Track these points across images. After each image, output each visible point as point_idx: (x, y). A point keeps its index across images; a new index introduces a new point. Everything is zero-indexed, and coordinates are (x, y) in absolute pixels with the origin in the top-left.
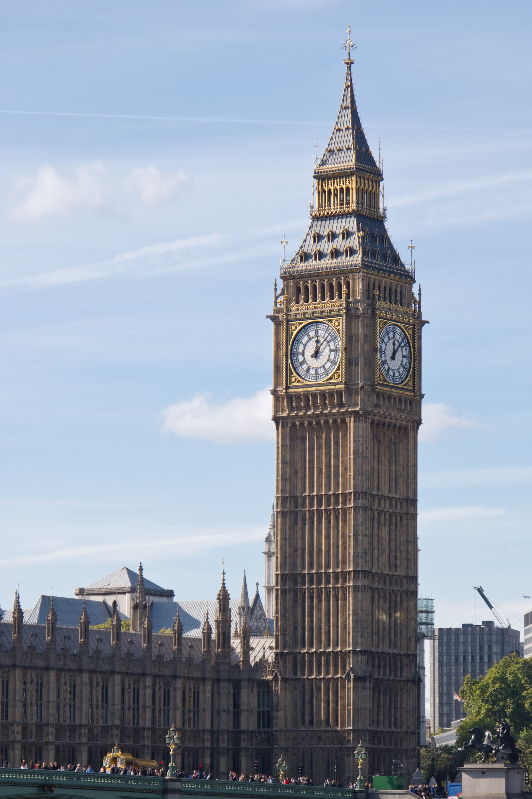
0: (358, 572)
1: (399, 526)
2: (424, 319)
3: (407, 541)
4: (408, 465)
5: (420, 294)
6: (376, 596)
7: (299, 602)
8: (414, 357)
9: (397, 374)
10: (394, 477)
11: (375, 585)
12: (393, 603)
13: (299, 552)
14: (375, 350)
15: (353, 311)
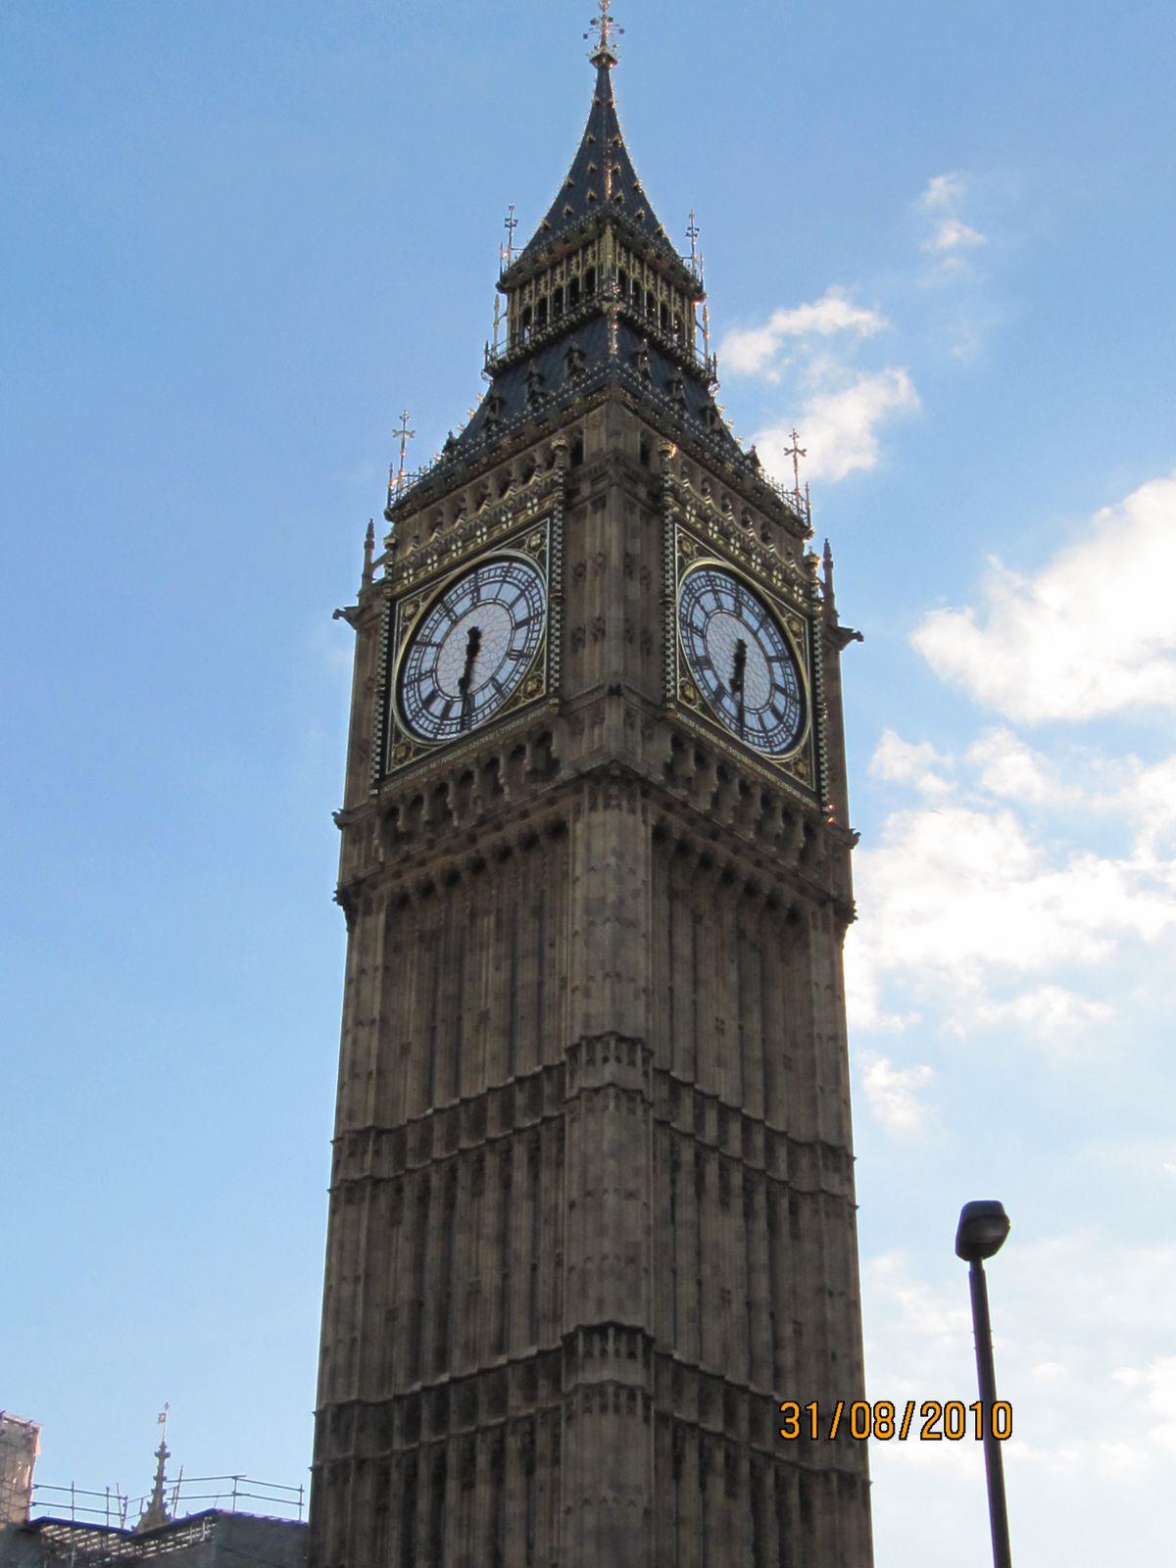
0: (601, 1330)
1: (785, 1228)
2: (841, 623)
3: (820, 1290)
4: (810, 1035)
5: (828, 565)
6: (691, 1458)
7: (395, 1506)
8: (815, 702)
9: (751, 720)
10: (758, 1053)
11: (688, 1413)
12: (771, 1508)
13: (404, 1318)
14: (665, 601)
15: (586, 490)
